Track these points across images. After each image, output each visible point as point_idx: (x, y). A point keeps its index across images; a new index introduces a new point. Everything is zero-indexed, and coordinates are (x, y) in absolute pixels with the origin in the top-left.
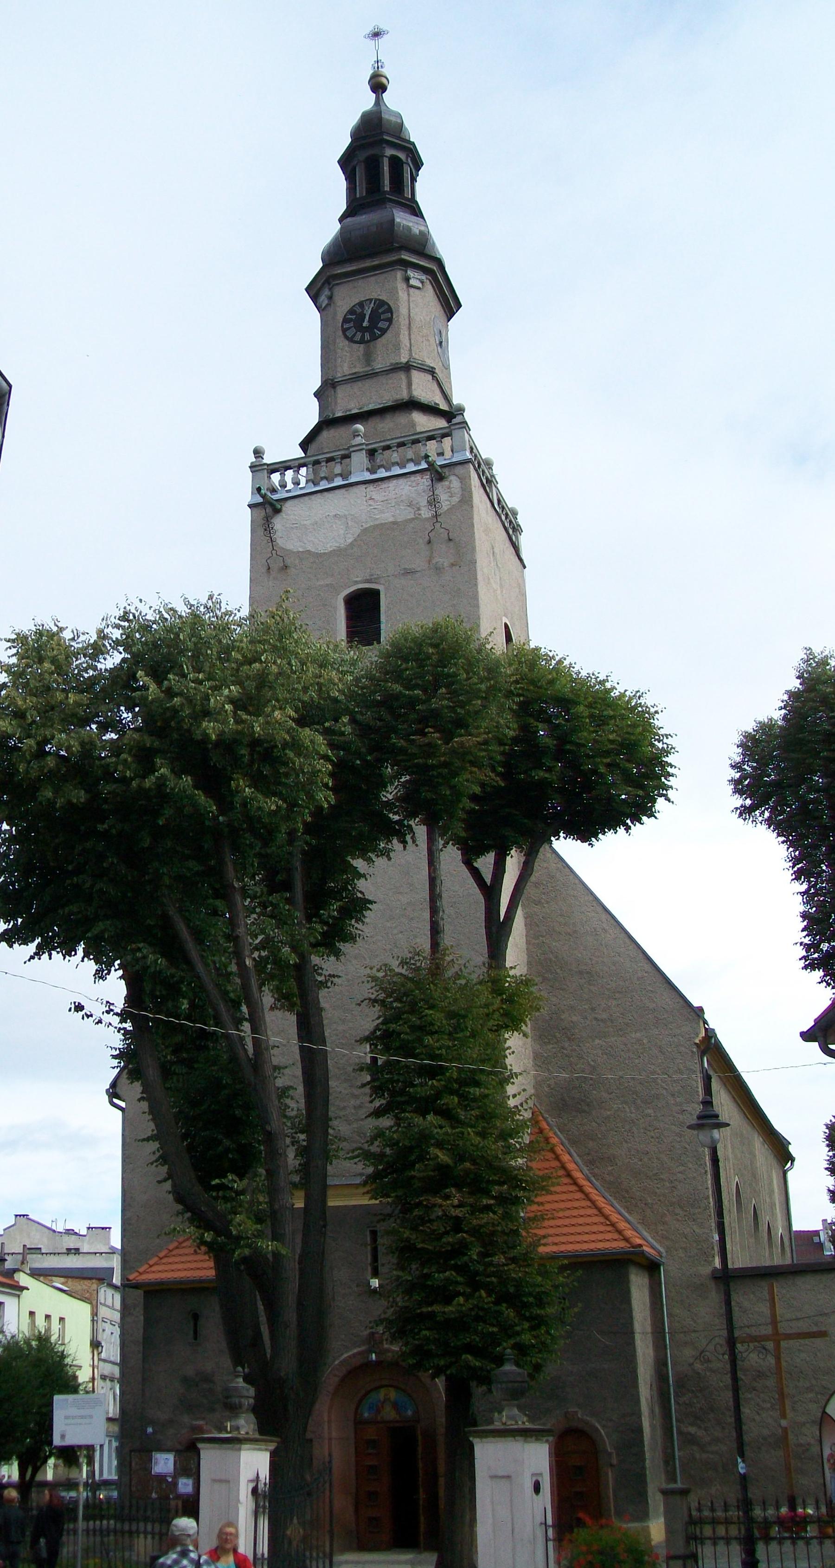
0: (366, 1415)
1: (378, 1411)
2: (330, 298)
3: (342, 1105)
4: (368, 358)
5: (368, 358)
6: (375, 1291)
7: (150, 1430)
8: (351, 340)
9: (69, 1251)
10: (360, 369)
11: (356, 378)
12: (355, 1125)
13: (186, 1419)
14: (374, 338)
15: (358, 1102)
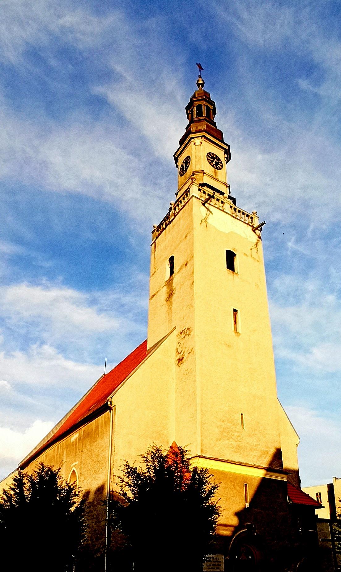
8: (210, 163)
10: (213, 174)
12: (238, 443)
15: (238, 435)
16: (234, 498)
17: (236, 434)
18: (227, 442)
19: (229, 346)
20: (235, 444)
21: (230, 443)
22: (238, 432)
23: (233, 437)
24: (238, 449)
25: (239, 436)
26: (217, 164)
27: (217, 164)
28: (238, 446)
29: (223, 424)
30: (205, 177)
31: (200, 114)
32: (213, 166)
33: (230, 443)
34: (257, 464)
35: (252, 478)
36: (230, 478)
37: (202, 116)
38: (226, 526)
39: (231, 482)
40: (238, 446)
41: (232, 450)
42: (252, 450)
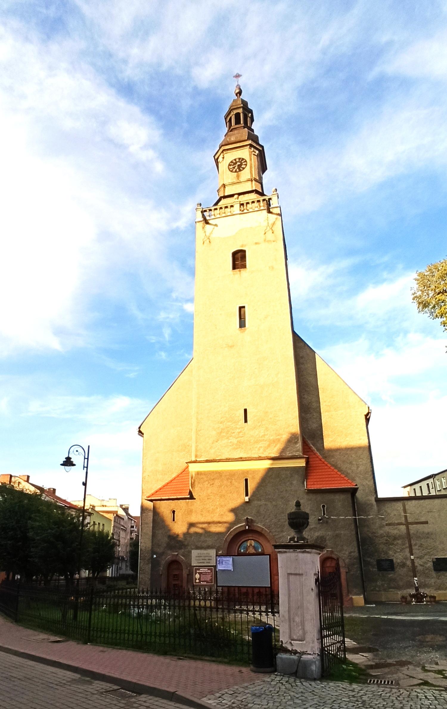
0: (242, 551)
1: (247, 550)
2: (223, 158)
3: (233, 431)
4: (238, 177)
5: (238, 177)
6: (247, 502)
7: (155, 556)
8: (232, 171)
9: (103, 506)
10: (235, 180)
11: (233, 184)
12: (239, 439)
13: (169, 552)
14: (240, 170)
15: (240, 430)
16: (230, 495)
17: (238, 430)
18: (226, 441)
19: (232, 347)
20: (235, 441)
21: (230, 441)
22: (239, 429)
23: (233, 435)
24: (239, 445)
25: (241, 432)
26: (239, 166)
27: (239, 166)
28: (239, 442)
29: (220, 425)
30: (227, 188)
31: (238, 122)
32: (236, 172)
33: (230, 441)
34: (263, 455)
35: (254, 472)
36: (226, 476)
37: (240, 123)
38: (219, 523)
39: (228, 479)
40: (239, 442)
41: (231, 447)
42: (257, 442)
